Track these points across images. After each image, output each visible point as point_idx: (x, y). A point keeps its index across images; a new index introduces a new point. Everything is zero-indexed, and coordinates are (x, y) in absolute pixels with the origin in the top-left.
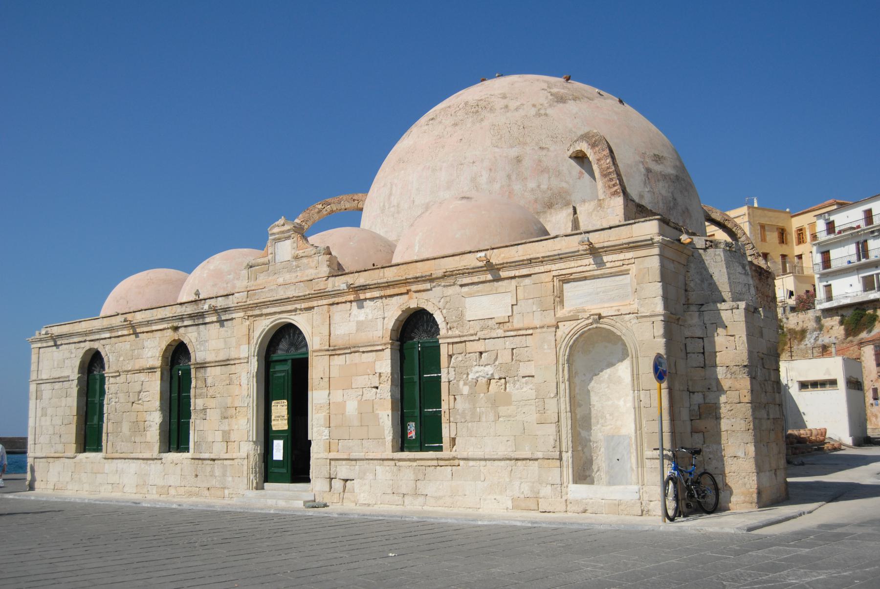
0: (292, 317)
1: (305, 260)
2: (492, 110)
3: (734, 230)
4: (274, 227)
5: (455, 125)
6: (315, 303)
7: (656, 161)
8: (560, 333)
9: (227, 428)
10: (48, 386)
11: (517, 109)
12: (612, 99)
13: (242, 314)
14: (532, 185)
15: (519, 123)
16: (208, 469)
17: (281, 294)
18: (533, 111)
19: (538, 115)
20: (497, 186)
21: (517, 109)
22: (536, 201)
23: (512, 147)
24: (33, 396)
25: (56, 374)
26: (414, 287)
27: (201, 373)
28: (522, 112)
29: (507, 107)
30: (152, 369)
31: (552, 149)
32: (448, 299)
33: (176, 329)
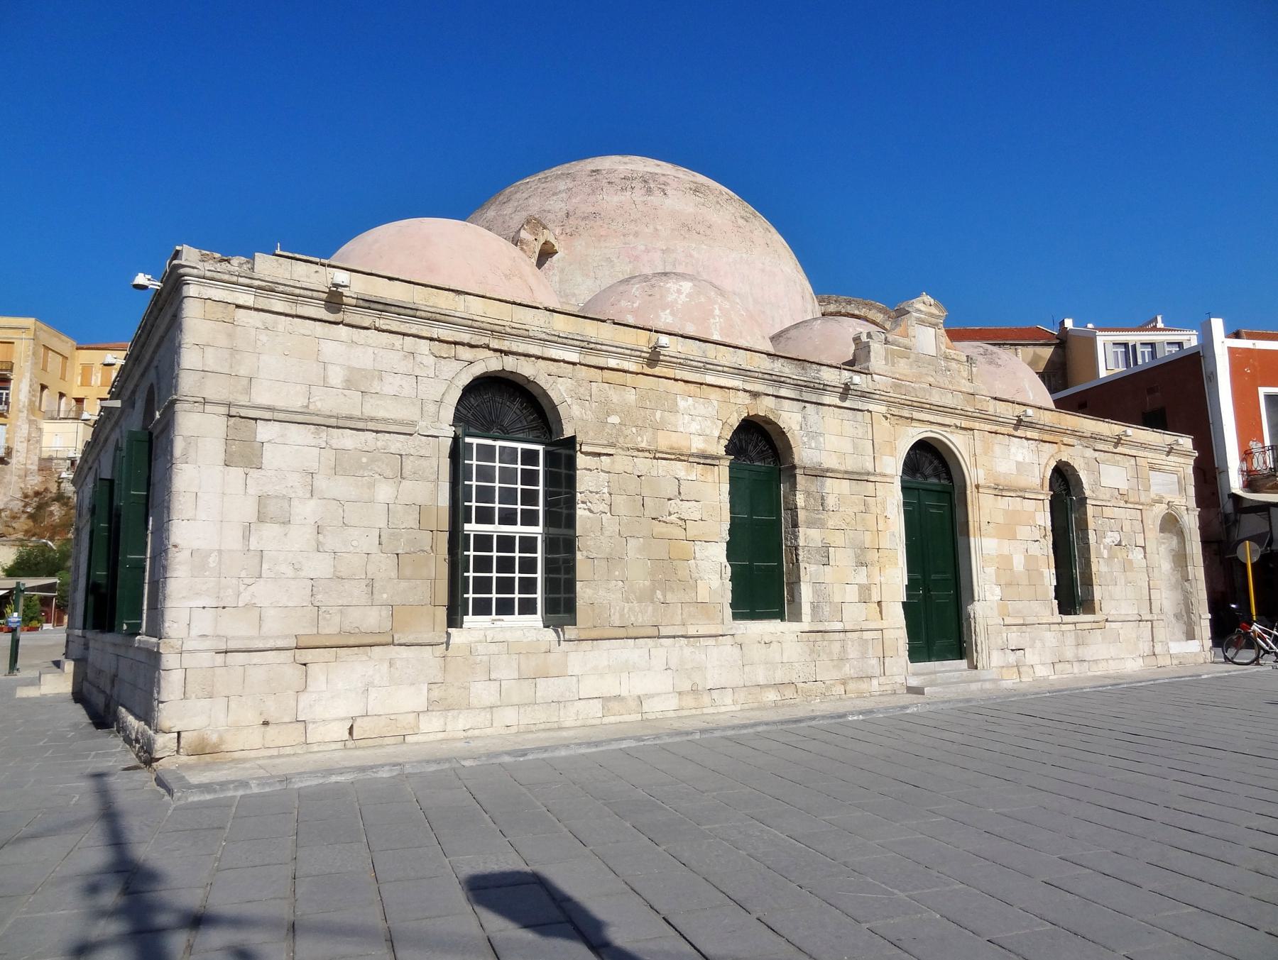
1: (954, 365)
6: (976, 425)
9: (864, 581)
13: (883, 409)
16: (836, 647)
17: (936, 398)
25: (349, 404)
26: (1066, 440)
27: (814, 485)
30: (706, 459)
33: (755, 395)
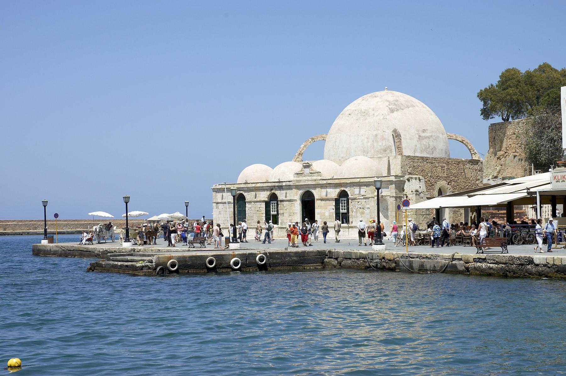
2: (369, 116)
14: (380, 144)
18: (382, 117)
19: (384, 118)
20: (369, 144)
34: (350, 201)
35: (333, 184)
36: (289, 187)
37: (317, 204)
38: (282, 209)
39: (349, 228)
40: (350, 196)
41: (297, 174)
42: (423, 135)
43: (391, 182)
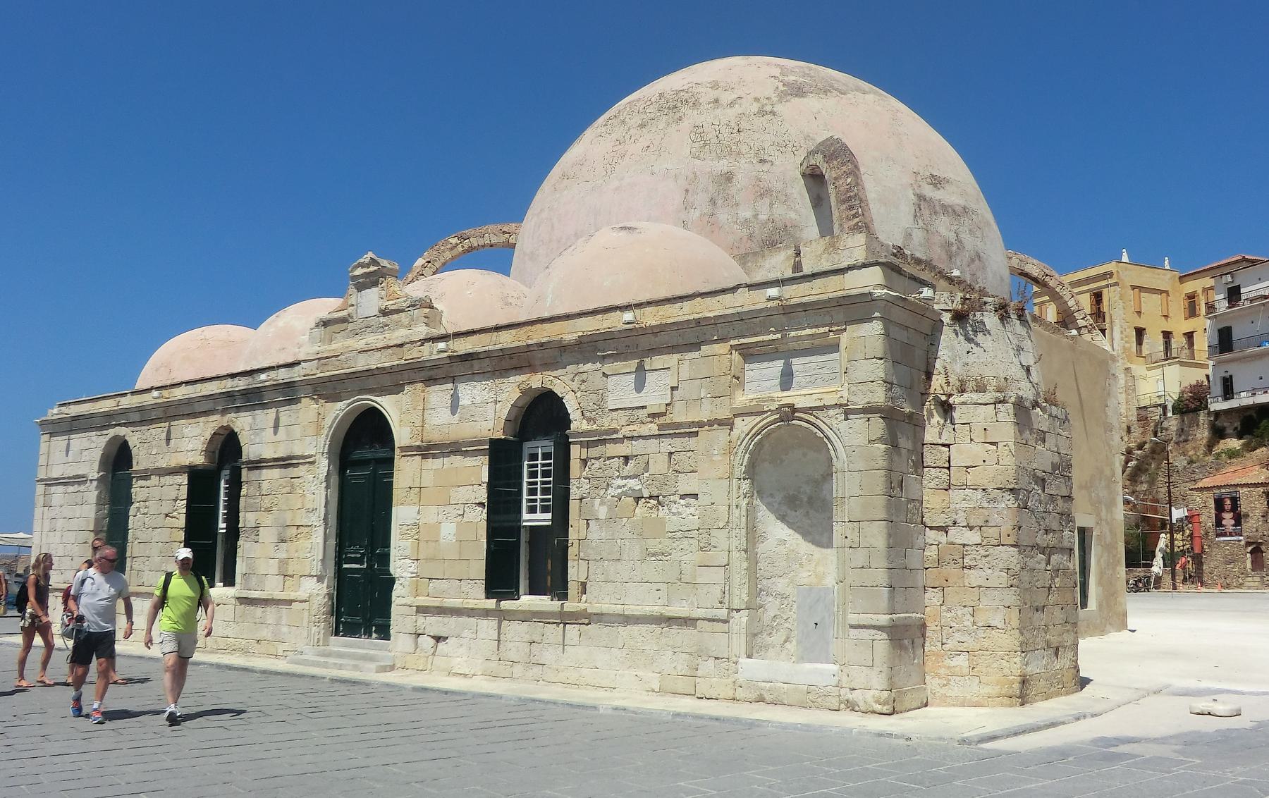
0: (378, 399)
2: (695, 105)
3: (1058, 290)
4: (357, 267)
5: (643, 126)
7: (935, 185)
8: (736, 432)
9: (284, 556)
10: (60, 489)
11: (731, 105)
12: (875, 93)
14: (746, 213)
15: (733, 125)
18: (755, 107)
21: (731, 105)
22: (751, 237)
23: (720, 158)
24: (40, 500)
27: (254, 475)
28: (737, 109)
29: (717, 101)
31: (777, 163)
32: (585, 376)
34: (576, 452)
35: (489, 355)
36: (289, 393)
37: (406, 472)
38: (257, 510)
39: (565, 619)
40: (578, 424)
41: (325, 323)
42: (929, 191)
43: (854, 308)
